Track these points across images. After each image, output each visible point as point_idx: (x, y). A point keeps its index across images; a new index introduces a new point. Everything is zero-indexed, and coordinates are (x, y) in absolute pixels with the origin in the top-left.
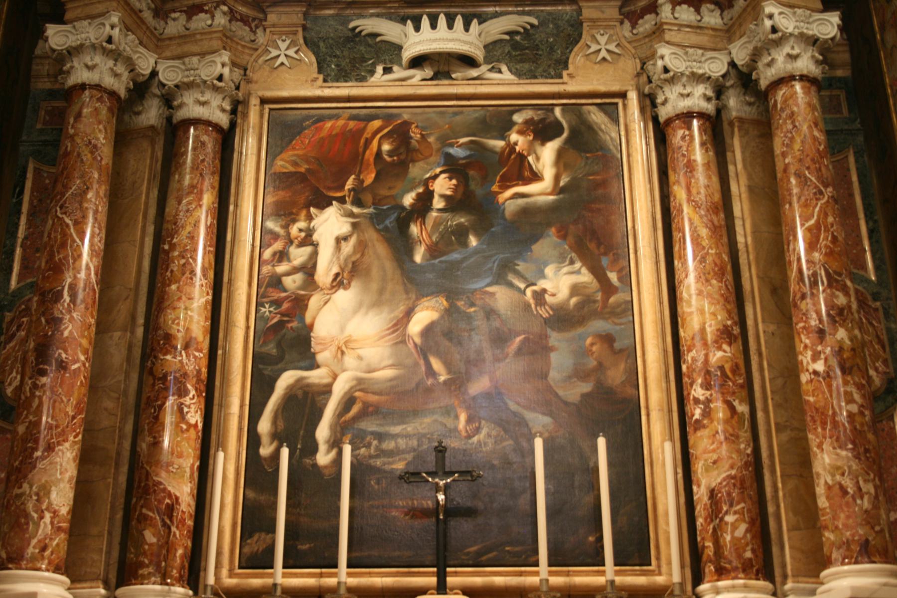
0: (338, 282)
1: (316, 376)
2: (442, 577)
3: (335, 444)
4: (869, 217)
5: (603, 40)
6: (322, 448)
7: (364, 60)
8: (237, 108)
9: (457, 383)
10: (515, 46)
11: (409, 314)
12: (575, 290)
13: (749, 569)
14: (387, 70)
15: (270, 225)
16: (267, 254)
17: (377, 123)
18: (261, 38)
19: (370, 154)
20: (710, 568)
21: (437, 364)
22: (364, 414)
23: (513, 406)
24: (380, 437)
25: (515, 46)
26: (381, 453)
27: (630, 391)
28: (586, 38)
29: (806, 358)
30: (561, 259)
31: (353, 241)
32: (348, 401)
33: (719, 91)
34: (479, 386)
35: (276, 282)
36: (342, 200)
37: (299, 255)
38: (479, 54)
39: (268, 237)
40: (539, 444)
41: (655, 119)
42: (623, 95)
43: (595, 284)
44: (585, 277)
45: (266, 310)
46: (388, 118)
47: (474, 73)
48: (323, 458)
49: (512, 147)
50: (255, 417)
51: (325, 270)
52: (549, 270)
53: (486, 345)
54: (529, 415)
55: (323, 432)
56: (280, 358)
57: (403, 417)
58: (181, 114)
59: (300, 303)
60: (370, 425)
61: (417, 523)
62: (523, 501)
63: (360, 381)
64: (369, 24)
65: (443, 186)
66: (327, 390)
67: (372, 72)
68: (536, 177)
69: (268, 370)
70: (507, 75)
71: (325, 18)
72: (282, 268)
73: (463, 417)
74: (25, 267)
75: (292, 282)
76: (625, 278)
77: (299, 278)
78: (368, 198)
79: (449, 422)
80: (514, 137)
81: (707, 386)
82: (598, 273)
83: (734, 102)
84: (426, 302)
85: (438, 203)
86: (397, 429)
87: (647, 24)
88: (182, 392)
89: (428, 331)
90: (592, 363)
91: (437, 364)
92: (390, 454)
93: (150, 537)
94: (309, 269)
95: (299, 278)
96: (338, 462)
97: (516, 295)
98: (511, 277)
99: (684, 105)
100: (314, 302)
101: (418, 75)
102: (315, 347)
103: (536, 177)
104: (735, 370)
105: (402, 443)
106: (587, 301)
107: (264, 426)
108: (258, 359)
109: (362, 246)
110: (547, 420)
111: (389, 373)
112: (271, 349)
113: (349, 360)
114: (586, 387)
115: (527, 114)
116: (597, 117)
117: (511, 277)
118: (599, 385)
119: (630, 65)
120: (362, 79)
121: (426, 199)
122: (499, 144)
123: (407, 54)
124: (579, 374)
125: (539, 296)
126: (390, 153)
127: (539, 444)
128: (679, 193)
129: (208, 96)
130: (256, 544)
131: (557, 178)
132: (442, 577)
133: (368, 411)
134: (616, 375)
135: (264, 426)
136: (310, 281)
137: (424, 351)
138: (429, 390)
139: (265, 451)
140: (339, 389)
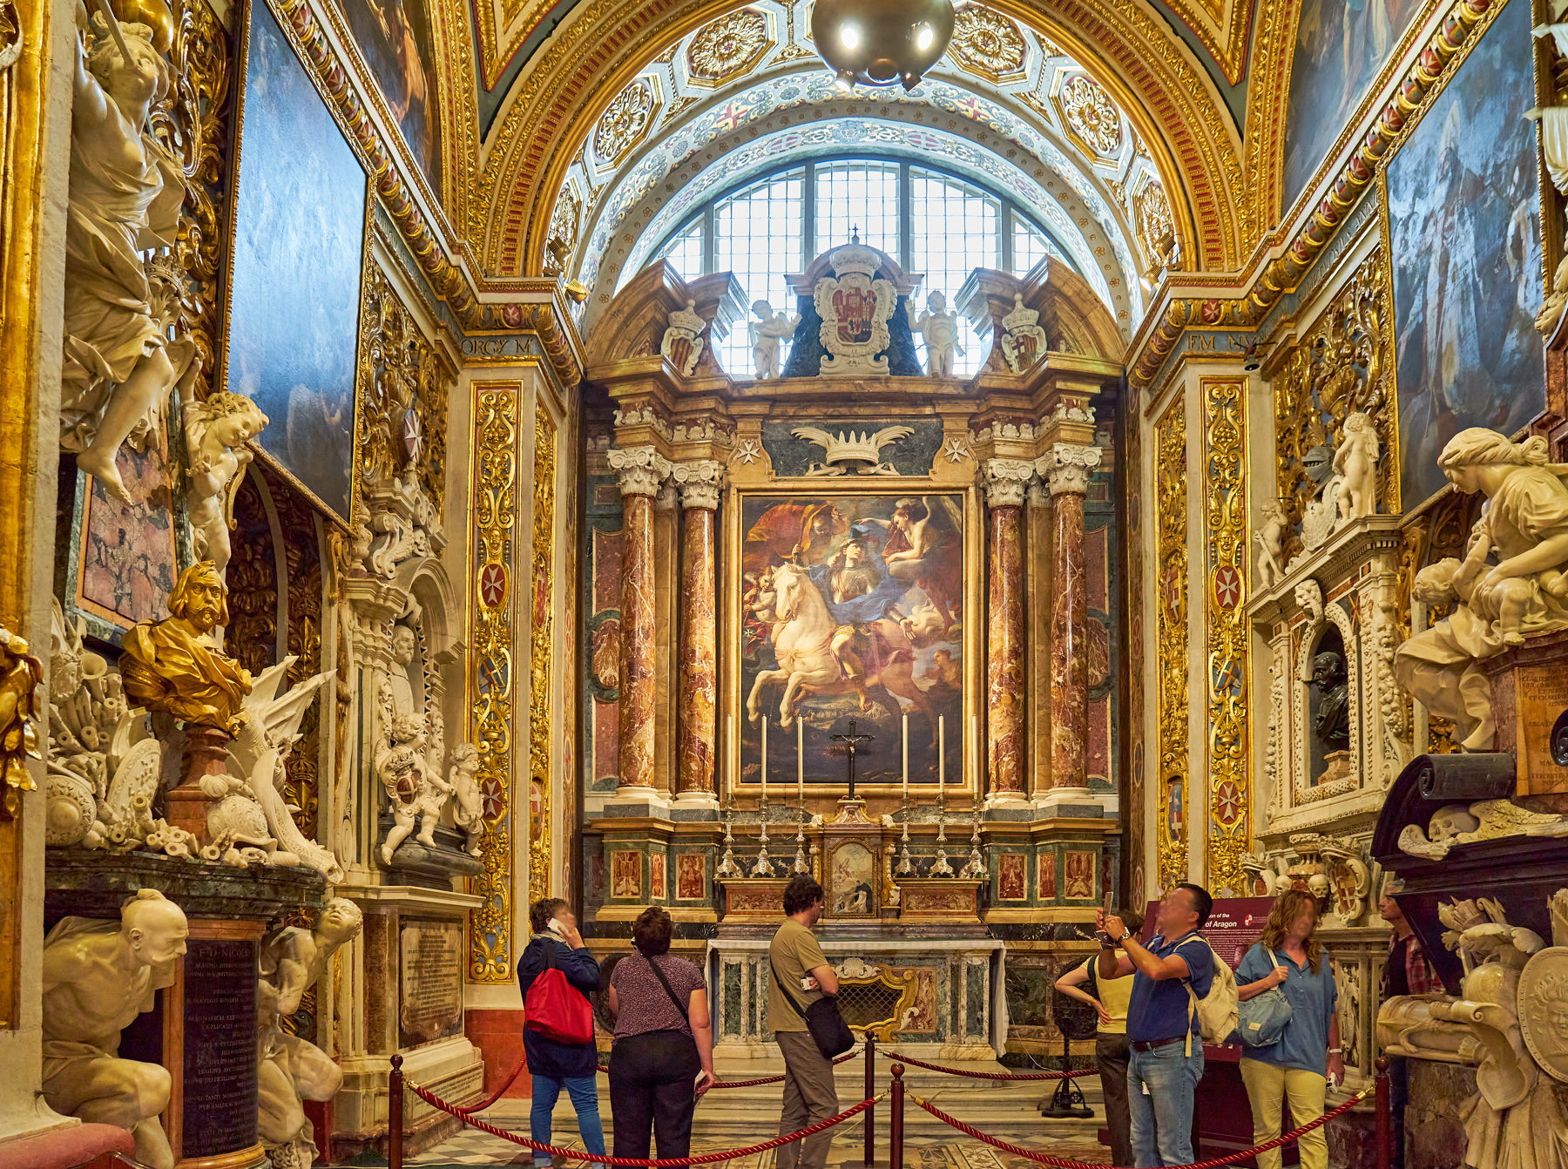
0: (790, 616)
1: (779, 674)
2: (852, 788)
3: (790, 714)
4: (1110, 573)
5: (956, 445)
6: (784, 716)
7: (801, 458)
8: (723, 493)
9: (859, 679)
10: (900, 449)
11: (832, 636)
12: (930, 621)
13: (1013, 785)
14: (817, 467)
15: (747, 577)
16: (747, 597)
17: (811, 507)
18: (734, 441)
19: (806, 530)
20: (993, 785)
21: (848, 668)
22: (806, 697)
23: (891, 693)
24: (817, 710)
25: (900, 449)
26: (816, 720)
27: (957, 685)
28: (945, 443)
29: (1054, 673)
30: (922, 602)
31: (798, 589)
32: (798, 690)
33: (1027, 488)
34: (871, 681)
35: (752, 614)
36: (790, 561)
37: (765, 598)
38: (875, 459)
39: (746, 586)
40: (905, 718)
41: (986, 503)
42: (966, 489)
43: (942, 619)
44: (936, 614)
45: (748, 633)
46: (818, 503)
47: (872, 470)
48: (785, 722)
49: (894, 525)
50: (745, 698)
51: (781, 611)
52: (915, 609)
53: (876, 656)
54: (899, 698)
55: (784, 708)
56: (756, 663)
57: (828, 699)
58: (687, 503)
59: (767, 629)
60: (810, 704)
61: (838, 758)
62: (895, 752)
63: (804, 677)
64: (805, 432)
65: (852, 551)
66: (785, 683)
67: (807, 468)
68: (909, 547)
69: (751, 670)
70: (894, 472)
71: (775, 425)
72: (755, 607)
73: (862, 699)
74: (599, 601)
75: (762, 616)
76: (959, 615)
77: (766, 612)
78: (805, 559)
79: (854, 702)
80: (896, 518)
81: (1000, 684)
82: (944, 612)
83: (1035, 497)
84: (842, 629)
85: (849, 564)
86: (825, 706)
87: (984, 435)
88: (704, 685)
89: (843, 647)
90: (937, 667)
91: (848, 668)
92: (822, 720)
93: (694, 766)
94: (772, 607)
95: (766, 612)
96: (794, 725)
97: (894, 626)
98: (892, 614)
99: (1003, 500)
100: (776, 627)
101: (836, 470)
102: (777, 656)
103: (909, 547)
104: (1017, 675)
105: (828, 714)
106: (935, 630)
107: (750, 703)
108: (746, 664)
109: (803, 592)
110: (909, 701)
111: (821, 673)
112: (752, 657)
113: (797, 665)
114: (933, 682)
115: (905, 502)
116: (949, 504)
117: (892, 614)
118: (940, 680)
119: (972, 465)
120: (801, 473)
121: (842, 559)
122: (886, 523)
123: (830, 458)
124: (929, 674)
125: (909, 625)
126: (820, 529)
127: (905, 718)
128: (996, 560)
129: (705, 490)
130: (750, 769)
131: (922, 547)
132: (852, 788)
133: (810, 695)
134: (950, 675)
135: (750, 703)
136: (773, 614)
137: (840, 660)
138: (844, 684)
139: (752, 718)
140: (792, 682)
